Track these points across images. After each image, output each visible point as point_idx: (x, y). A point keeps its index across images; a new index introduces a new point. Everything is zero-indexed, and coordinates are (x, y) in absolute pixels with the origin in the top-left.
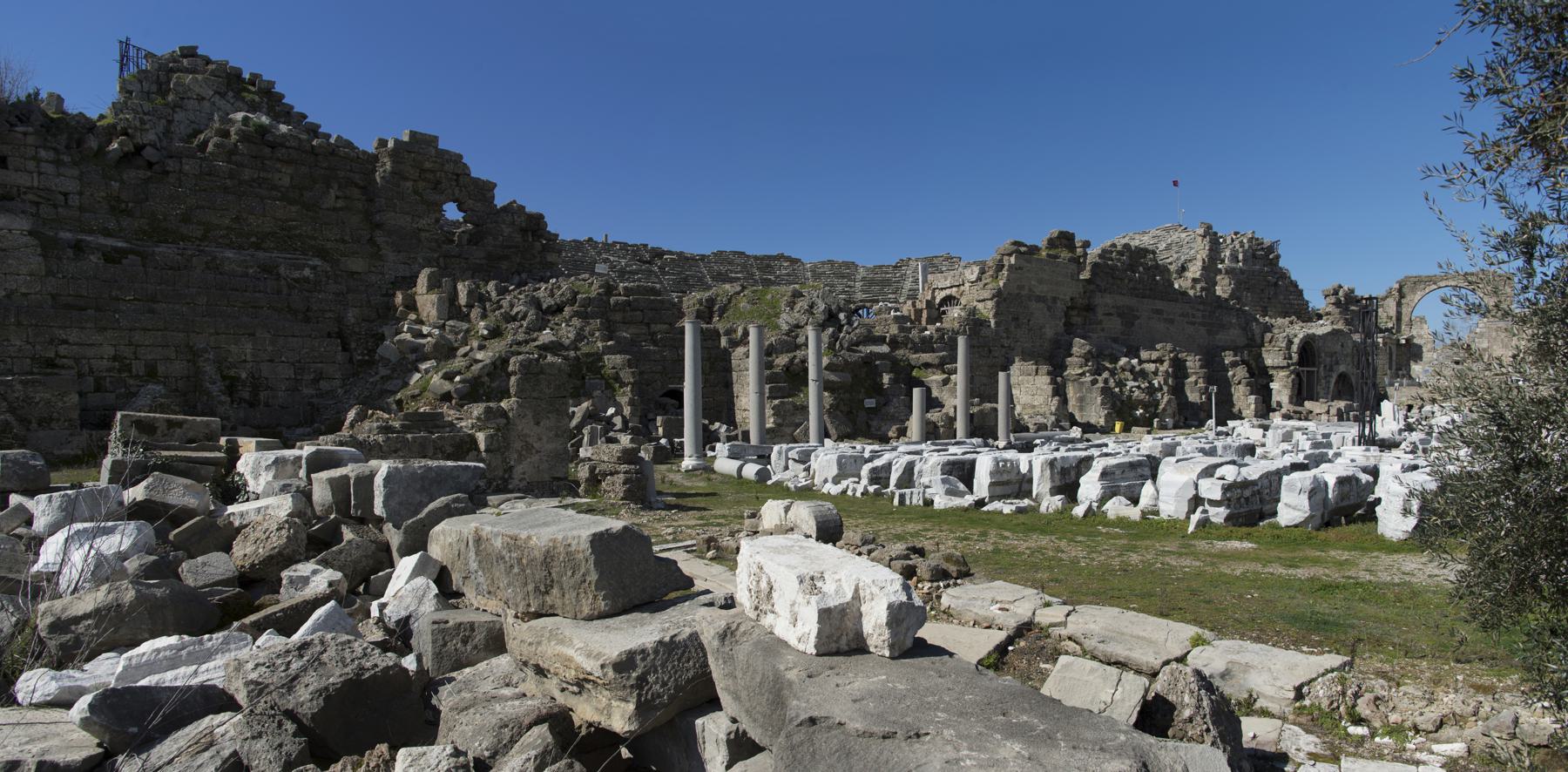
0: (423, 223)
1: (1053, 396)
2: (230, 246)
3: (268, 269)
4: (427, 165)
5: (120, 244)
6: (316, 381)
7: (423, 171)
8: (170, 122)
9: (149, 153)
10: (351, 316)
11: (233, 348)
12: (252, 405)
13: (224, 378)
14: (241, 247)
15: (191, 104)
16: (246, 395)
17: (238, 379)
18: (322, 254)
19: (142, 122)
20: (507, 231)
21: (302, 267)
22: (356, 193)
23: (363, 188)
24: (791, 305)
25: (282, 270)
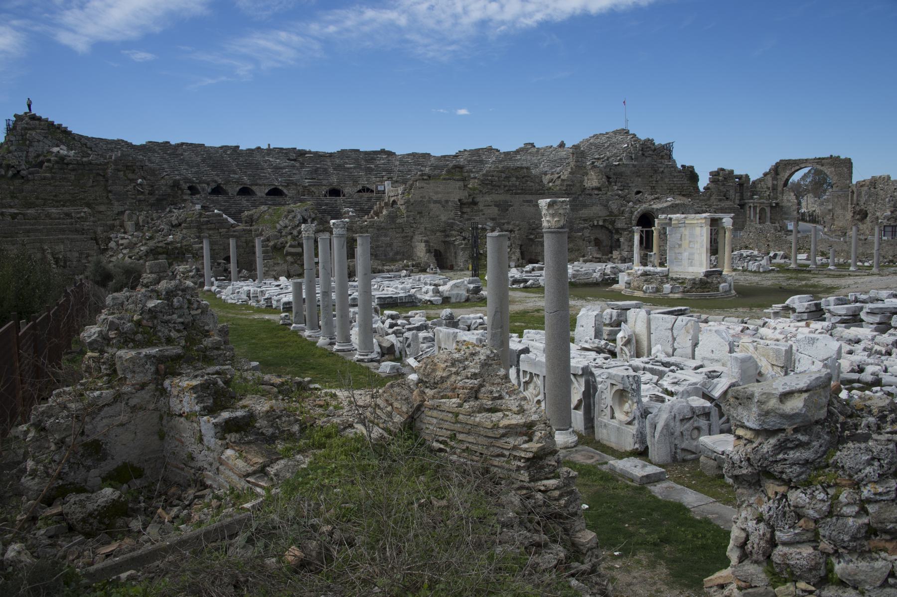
1: (426, 253)
2: (53, 206)
3: (68, 215)
4: (129, 164)
5: (16, 211)
6: (87, 257)
7: (127, 166)
8: (27, 152)
9: (23, 173)
10: (99, 230)
11: (57, 248)
12: (64, 267)
13: (54, 258)
14: (58, 207)
15: (36, 144)
16: (62, 264)
17: (59, 258)
18: (88, 205)
19: (19, 162)
20: (164, 188)
21: (80, 213)
22: (101, 178)
23: (104, 176)
24: (286, 217)
25: (73, 215)
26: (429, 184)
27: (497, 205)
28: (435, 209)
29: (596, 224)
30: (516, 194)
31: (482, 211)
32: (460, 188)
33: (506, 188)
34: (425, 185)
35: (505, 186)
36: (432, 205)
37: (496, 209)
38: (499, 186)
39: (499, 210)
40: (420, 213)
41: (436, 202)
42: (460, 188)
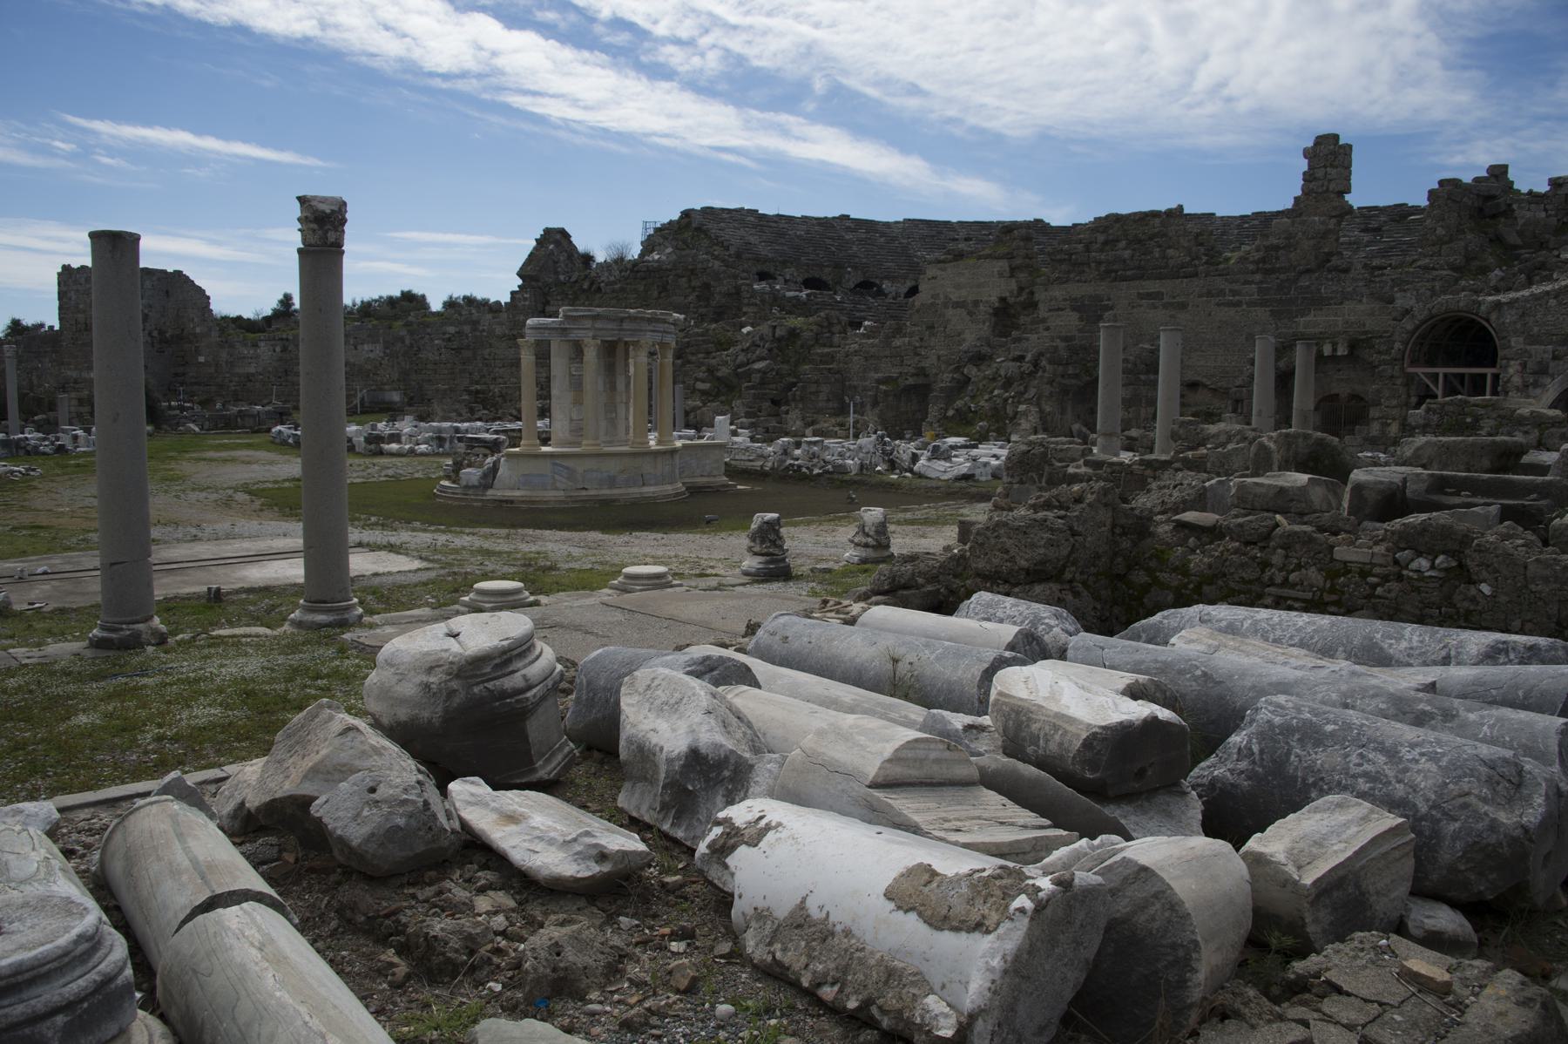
0: (690, 298)
26: (944, 270)
27: (1078, 306)
28: (955, 317)
29: (1327, 350)
30: (1125, 279)
31: (1044, 320)
32: (1001, 275)
33: (1103, 268)
34: (939, 273)
35: (1099, 263)
36: (950, 312)
37: (1075, 315)
38: (1088, 265)
39: (1081, 319)
40: (931, 327)
41: (957, 305)
42: (1001, 275)
